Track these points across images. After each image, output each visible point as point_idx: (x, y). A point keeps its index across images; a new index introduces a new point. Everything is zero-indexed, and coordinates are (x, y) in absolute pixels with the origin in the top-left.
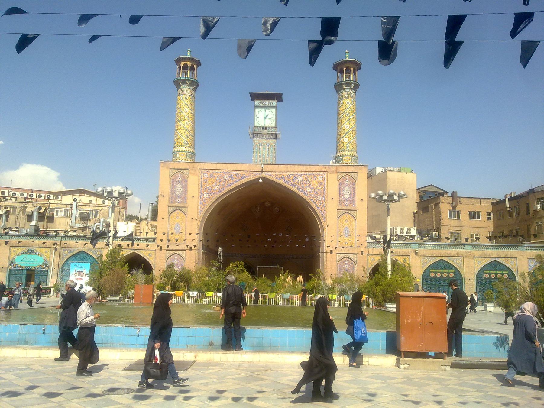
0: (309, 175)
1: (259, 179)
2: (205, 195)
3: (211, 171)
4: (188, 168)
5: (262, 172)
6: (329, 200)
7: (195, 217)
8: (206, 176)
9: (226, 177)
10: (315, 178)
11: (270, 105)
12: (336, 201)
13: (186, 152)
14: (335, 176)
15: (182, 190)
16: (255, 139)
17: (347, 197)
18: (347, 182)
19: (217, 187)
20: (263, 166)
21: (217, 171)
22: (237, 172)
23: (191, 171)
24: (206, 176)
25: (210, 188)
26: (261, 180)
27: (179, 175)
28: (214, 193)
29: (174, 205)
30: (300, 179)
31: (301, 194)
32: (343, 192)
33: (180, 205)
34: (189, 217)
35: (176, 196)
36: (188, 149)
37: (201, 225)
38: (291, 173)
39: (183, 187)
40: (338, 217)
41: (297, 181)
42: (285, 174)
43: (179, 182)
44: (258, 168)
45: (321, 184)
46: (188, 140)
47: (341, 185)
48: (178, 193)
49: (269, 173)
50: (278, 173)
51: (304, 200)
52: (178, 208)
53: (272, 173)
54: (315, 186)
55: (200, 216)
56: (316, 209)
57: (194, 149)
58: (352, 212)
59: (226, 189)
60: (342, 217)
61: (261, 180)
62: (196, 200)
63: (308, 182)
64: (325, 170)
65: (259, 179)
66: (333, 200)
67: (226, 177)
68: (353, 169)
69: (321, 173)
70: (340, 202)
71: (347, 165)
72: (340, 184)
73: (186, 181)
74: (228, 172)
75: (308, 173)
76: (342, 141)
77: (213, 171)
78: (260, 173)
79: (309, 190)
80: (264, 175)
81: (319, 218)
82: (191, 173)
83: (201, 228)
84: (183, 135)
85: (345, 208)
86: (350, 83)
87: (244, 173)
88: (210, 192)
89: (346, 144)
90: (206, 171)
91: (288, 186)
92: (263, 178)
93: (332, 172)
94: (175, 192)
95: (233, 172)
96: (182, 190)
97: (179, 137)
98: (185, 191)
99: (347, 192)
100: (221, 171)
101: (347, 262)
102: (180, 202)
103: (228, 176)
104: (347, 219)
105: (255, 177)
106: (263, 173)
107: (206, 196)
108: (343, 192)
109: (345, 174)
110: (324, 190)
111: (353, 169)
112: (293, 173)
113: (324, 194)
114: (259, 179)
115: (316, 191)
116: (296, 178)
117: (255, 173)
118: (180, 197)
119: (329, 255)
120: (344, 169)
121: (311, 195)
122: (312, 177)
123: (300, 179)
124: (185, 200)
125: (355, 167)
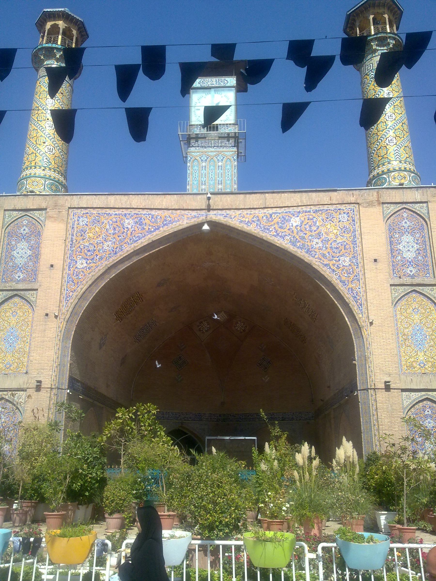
0: (316, 212)
1: (202, 224)
2: (79, 262)
3: (95, 212)
4: (44, 206)
5: (209, 209)
6: (369, 265)
7: (53, 309)
8: (83, 221)
9: (129, 223)
10: (329, 218)
11: (222, 84)
12: (384, 266)
13: (44, 177)
14: (377, 211)
15: (29, 252)
16: (192, 149)
17: (410, 255)
18: (406, 224)
19: (108, 246)
20: (209, 195)
21: (108, 211)
22: (153, 212)
23: (51, 212)
24: (83, 221)
25: (91, 248)
26: (206, 227)
27: (25, 222)
28: (101, 258)
29: (8, 286)
30: (295, 221)
31: (301, 254)
32: (401, 247)
33: (20, 286)
34: (40, 312)
35: (15, 266)
36: (48, 173)
37: (67, 330)
38: (274, 210)
39: (31, 248)
40: (396, 303)
41: (288, 225)
42: (260, 213)
43: (25, 238)
44: (200, 202)
45: (345, 230)
46: (50, 156)
47: (393, 233)
48: (20, 261)
49: (223, 212)
50: (245, 212)
51: (309, 266)
52: (16, 294)
53: (231, 212)
54: (331, 236)
55: (66, 309)
56: (340, 287)
57: (65, 178)
58: (426, 290)
59: (128, 249)
60: (403, 302)
61: (206, 227)
62: (57, 274)
63: (314, 228)
64: (353, 199)
65: (202, 224)
66: (379, 265)
67: (129, 223)
68: (417, 196)
69: (343, 207)
70: (396, 267)
71: (401, 187)
72: (391, 230)
73: (39, 234)
74: (134, 212)
75: (313, 208)
76: (383, 144)
77: (100, 211)
78: (203, 212)
79: (317, 243)
80: (214, 216)
81: (346, 305)
82: (50, 217)
83: (65, 338)
84: (41, 147)
85: (408, 281)
86: (385, 38)
87: (167, 213)
88: (90, 254)
89: (392, 149)
90: (84, 211)
91: (269, 236)
92: (210, 223)
93: (370, 204)
94: (12, 258)
95: (145, 212)
96: (29, 252)
97: (32, 150)
98: (36, 256)
99: (408, 246)
100: (117, 212)
101: (428, 412)
102: (24, 280)
103: (131, 221)
104: (415, 305)
105: (193, 221)
106: (212, 212)
107: (81, 264)
108: (401, 247)
109: (400, 207)
110: (354, 242)
111: (417, 196)
112: (279, 210)
113: (355, 252)
114: (202, 224)
115: (334, 245)
116: (285, 220)
117: (194, 213)
118: (23, 268)
119: (381, 396)
120: (397, 196)
121: (324, 255)
122: (324, 216)
123: (295, 221)
124: (33, 274)
125: (420, 191)
